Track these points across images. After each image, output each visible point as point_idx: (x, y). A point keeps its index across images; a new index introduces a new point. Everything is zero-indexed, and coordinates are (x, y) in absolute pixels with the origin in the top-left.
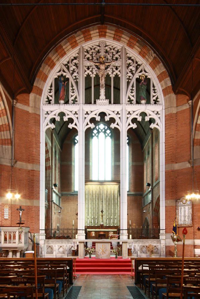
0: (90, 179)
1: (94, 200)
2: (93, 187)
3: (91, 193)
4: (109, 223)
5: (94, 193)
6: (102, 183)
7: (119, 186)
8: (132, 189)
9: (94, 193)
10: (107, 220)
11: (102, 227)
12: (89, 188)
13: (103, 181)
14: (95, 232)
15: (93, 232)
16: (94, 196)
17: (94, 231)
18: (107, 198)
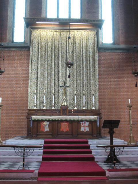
0: (43, 16)
1: (49, 59)
2: (46, 34)
3: (43, 45)
4: (78, 105)
5: (49, 44)
6: (64, 24)
7: (97, 32)
8: (122, 39)
9: (49, 44)
10: (74, 98)
11: (65, 110)
12: (40, 36)
13: (66, 20)
14: (51, 122)
15: (45, 123)
16: (49, 50)
17: (48, 121)
18: (75, 55)
